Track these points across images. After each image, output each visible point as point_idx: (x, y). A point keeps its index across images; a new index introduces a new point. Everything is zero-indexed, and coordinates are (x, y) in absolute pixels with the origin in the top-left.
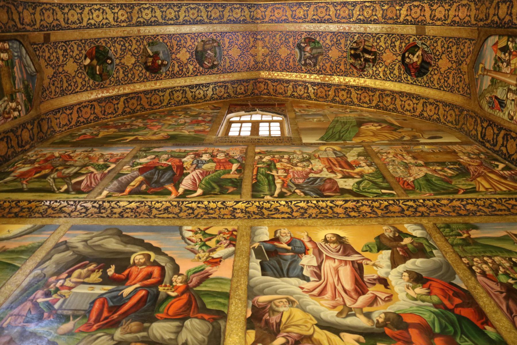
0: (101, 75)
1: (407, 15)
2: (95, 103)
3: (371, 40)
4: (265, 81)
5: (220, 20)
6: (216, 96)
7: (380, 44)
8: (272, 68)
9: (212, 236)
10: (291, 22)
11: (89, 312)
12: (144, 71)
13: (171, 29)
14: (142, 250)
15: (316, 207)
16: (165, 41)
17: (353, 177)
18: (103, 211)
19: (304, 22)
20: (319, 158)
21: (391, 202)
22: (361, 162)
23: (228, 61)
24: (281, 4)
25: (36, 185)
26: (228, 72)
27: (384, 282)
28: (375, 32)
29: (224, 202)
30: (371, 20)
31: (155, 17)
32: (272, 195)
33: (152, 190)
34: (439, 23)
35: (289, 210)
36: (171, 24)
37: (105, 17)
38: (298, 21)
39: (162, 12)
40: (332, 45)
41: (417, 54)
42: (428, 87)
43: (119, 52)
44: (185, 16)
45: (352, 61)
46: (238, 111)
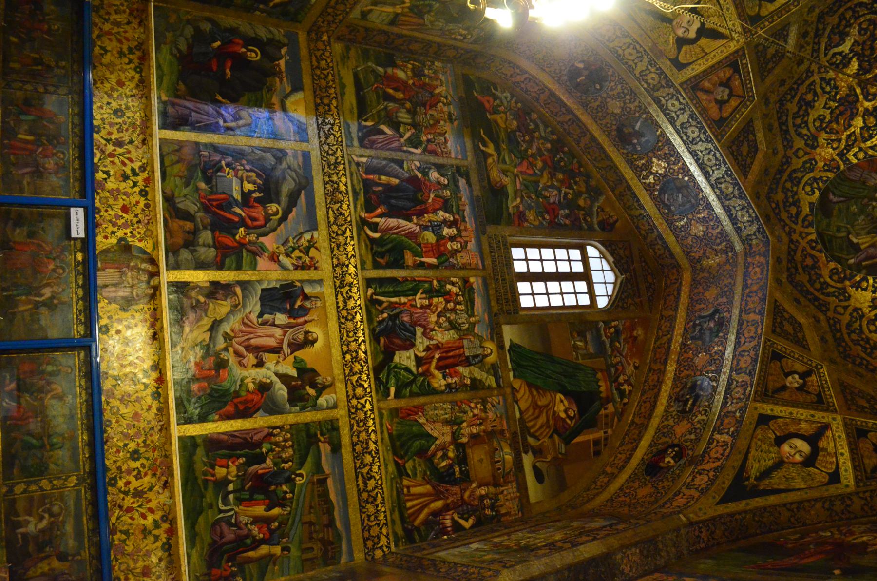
0: (578, 84)
1: (718, 442)
2: (547, 91)
4: (679, 280)
5: (722, 198)
6: (635, 220)
7: (699, 416)
8: (695, 283)
9: (307, 253)
10: (743, 295)
11: (216, 194)
12: (614, 127)
13: (676, 141)
14: (282, 209)
15: (356, 329)
16: (661, 139)
17: (418, 367)
18: (332, 167)
19: (741, 312)
20: (461, 339)
21: (368, 390)
22: (456, 379)
23: (682, 223)
25: (371, 97)
26: (670, 227)
27: (260, 364)
29: (354, 256)
31: (678, 116)
32: (374, 294)
33: (373, 197)
35: (349, 307)
36: (681, 138)
37: (636, 61)
38: (744, 303)
39: (688, 122)
40: (711, 355)
41: (672, 461)
42: (630, 477)
43: (615, 92)
44: (701, 152)
45: (689, 385)
46: (612, 255)
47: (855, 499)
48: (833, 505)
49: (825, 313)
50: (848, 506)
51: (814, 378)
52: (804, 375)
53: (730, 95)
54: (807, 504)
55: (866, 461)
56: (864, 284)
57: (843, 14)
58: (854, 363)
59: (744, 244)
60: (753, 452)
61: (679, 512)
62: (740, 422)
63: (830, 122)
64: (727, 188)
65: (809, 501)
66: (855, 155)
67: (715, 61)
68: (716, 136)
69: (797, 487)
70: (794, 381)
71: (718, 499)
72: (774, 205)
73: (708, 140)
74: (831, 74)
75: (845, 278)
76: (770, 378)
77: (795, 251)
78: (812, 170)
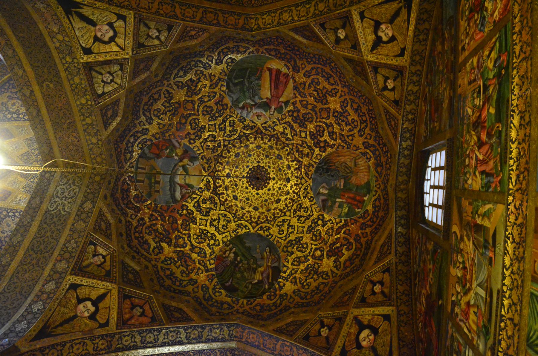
10: (263, 350)
36: (150, 347)
39: (142, 337)
47: (400, 308)
48: (403, 321)
49: (290, 308)
50: (405, 313)
51: (325, 320)
52: (323, 325)
53: (141, 307)
54: (401, 335)
55: (380, 299)
56: (282, 284)
57: (135, 237)
58: (323, 300)
59: (233, 341)
63: (187, 269)
64: (194, 334)
65: (399, 334)
66: (211, 265)
67: (116, 305)
68: (160, 325)
69: (389, 340)
72: (217, 314)
73: (160, 331)
74: (163, 258)
75: (275, 293)
76: (319, 344)
77: (249, 313)
78: (208, 288)
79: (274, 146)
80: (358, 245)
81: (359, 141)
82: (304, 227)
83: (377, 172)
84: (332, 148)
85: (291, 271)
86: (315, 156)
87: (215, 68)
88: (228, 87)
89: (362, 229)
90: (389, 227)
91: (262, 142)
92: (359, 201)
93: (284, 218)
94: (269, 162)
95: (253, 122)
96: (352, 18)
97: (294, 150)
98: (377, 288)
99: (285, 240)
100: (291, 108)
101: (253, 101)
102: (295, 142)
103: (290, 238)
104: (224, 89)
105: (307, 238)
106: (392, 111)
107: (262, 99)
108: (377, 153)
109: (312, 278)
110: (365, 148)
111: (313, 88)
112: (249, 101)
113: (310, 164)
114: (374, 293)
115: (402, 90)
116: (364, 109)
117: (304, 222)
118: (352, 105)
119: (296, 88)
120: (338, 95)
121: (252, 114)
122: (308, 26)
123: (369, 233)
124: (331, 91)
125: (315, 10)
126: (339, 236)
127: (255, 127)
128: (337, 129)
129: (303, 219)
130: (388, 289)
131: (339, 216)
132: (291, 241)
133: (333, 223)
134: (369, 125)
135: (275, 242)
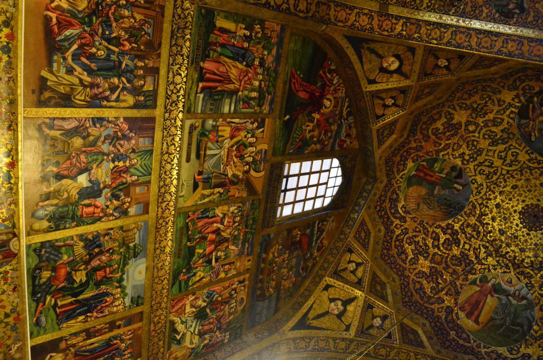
1: (396, 24)
3: (436, 6)
10: (525, 38)
19: (509, 35)
24: (532, 60)
28: (431, 13)
30: (433, 25)
34: (366, 11)
38: (516, 38)
40: (481, 6)
49: (501, 77)
51: (445, 71)
52: (447, 68)
56: (517, 100)
60: (388, 45)
61: (327, 24)
62: (410, 37)
69: (365, 67)
70: (443, 62)
71: (349, 34)
76: (445, 53)
79: (504, 245)
80: (425, 132)
81: (409, 224)
82: (486, 155)
83: (397, 195)
84: (439, 225)
85: (505, 112)
86: (461, 223)
87: (534, 353)
88: (530, 327)
89: (421, 146)
90: (380, 151)
91: (517, 254)
92: (422, 171)
93: (510, 169)
94: (516, 230)
95: (519, 279)
96: (357, 330)
97: (482, 234)
98: (390, 102)
99: (512, 145)
100: (470, 277)
101: (509, 300)
102: (479, 242)
103: (504, 146)
104: (535, 327)
105: (484, 144)
106: (356, 246)
107: (498, 298)
108: (393, 211)
109: (480, 104)
110: (405, 217)
111: (440, 286)
112: (514, 302)
113: (469, 217)
114: (392, 98)
115: (339, 260)
116: (394, 251)
117: (486, 160)
118: (407, 258)
119: (458, 293)
120: (417, 271)
121: (516, 287)
122: (404, 343)
123: (413, 142)
124: (423, 276)
125: (389, 352)
126: (447, 142)
127: (518, 273)
128: (429, 242)
129: (487, 163)
130: (375, 102)
131: (445, 160)
132: (502, 143)
133: (452, 155)
134: (395, 237)
135: (523, 145)
